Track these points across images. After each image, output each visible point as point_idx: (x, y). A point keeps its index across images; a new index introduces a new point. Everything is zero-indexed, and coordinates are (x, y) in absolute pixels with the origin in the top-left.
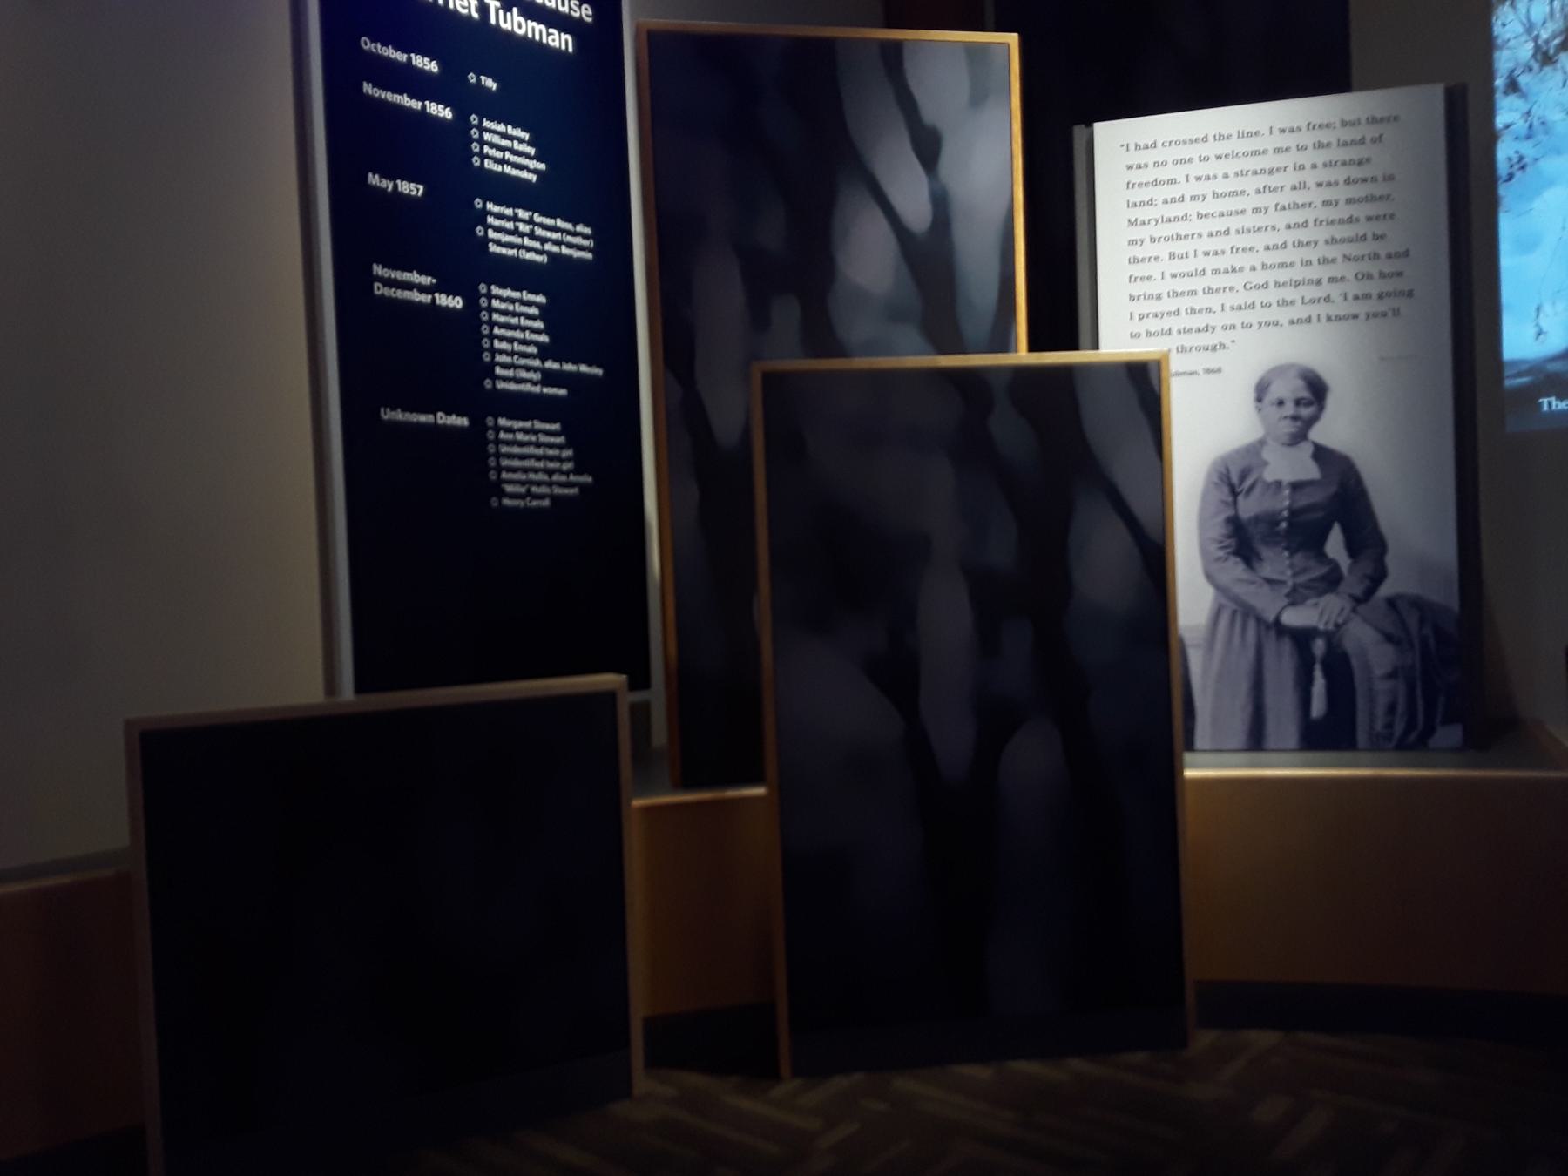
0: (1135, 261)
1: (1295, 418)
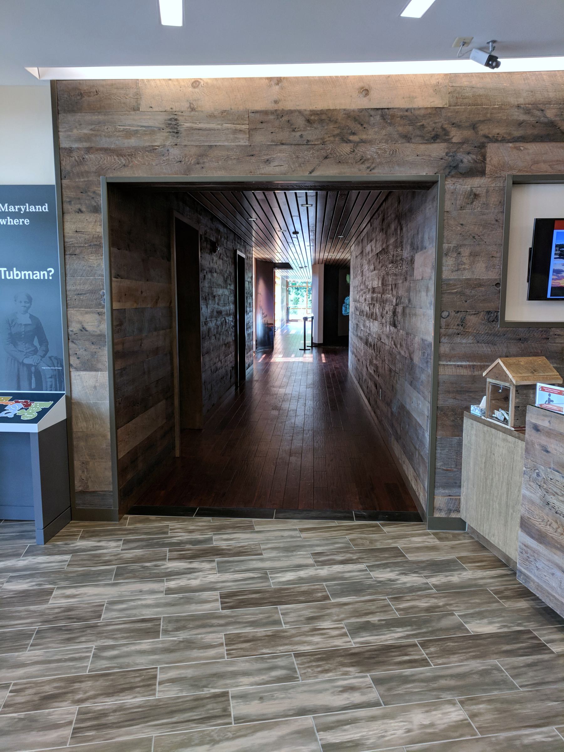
1: (25, 307)
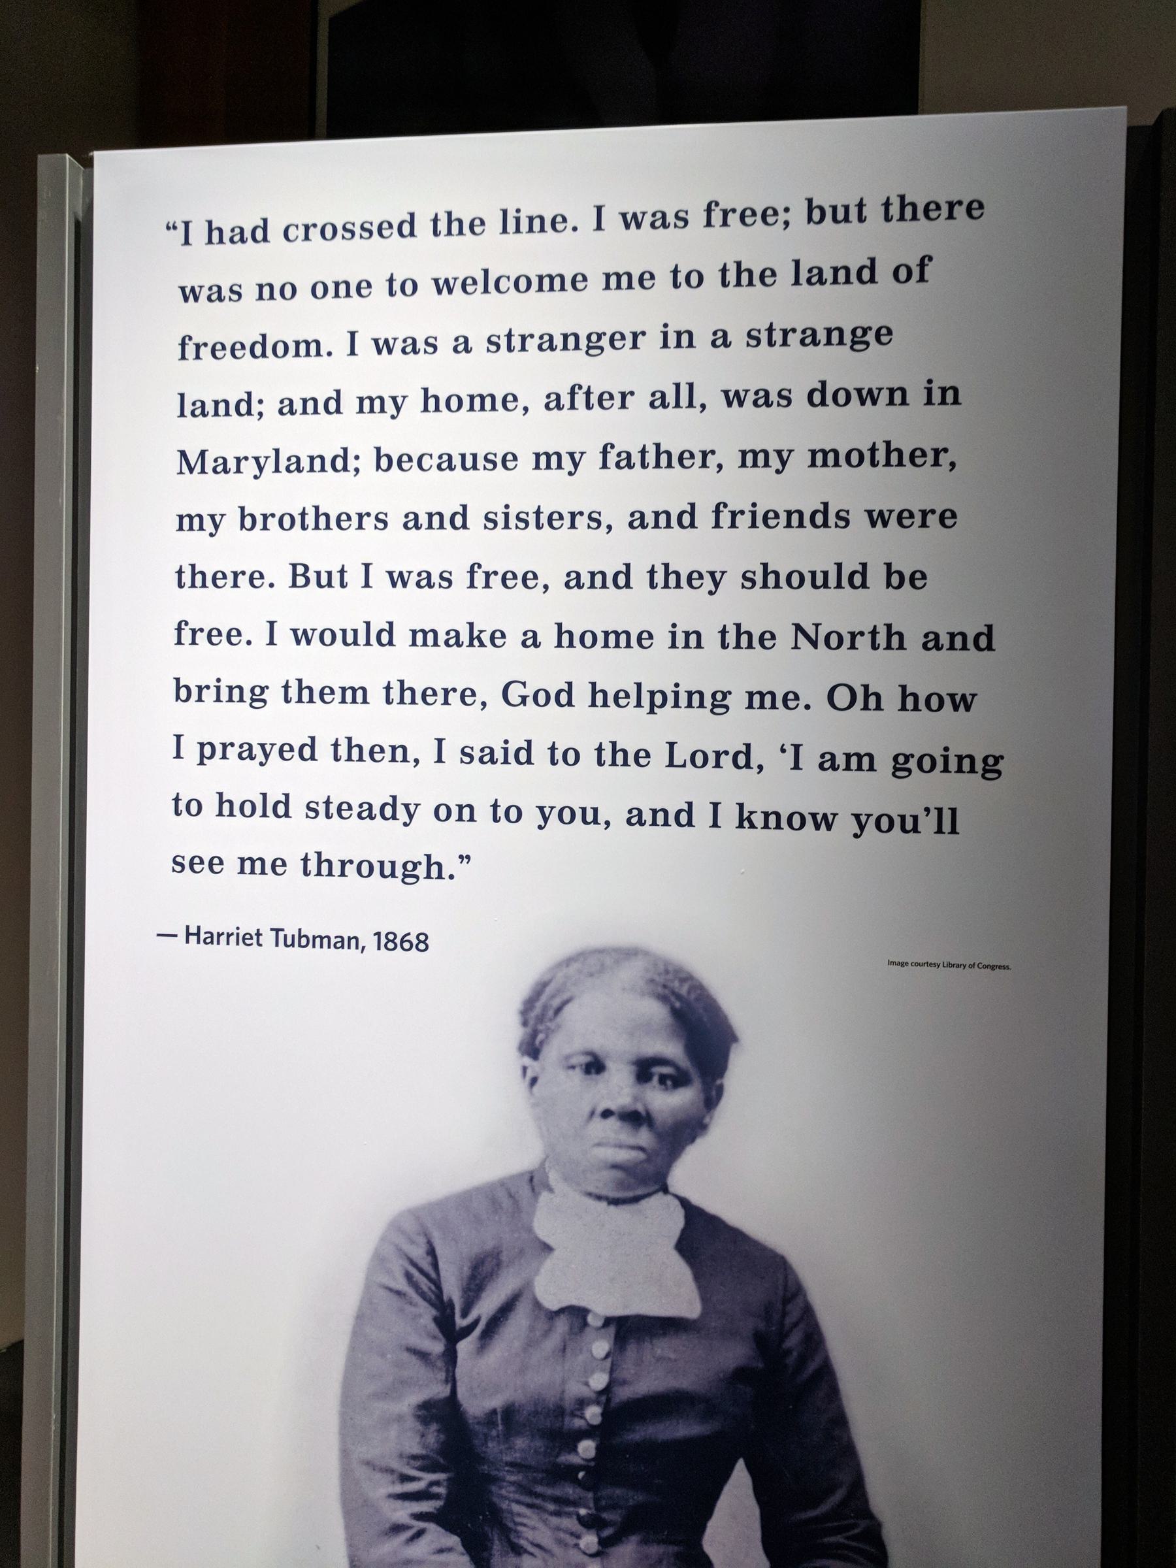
0: (193, 577)
1: (634, 1118)
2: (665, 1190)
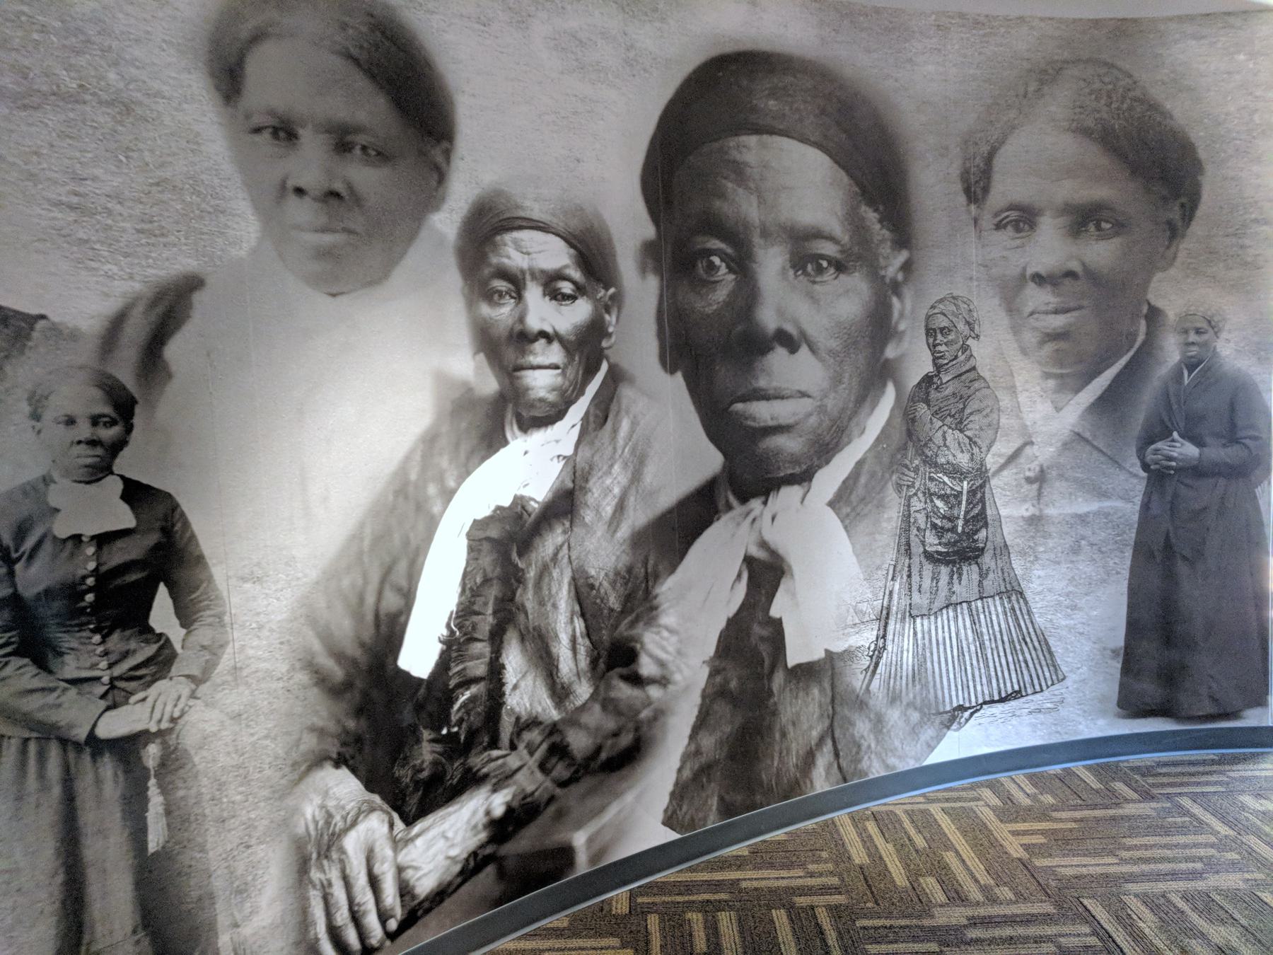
1: (93, 443)
2: (112, 473)
